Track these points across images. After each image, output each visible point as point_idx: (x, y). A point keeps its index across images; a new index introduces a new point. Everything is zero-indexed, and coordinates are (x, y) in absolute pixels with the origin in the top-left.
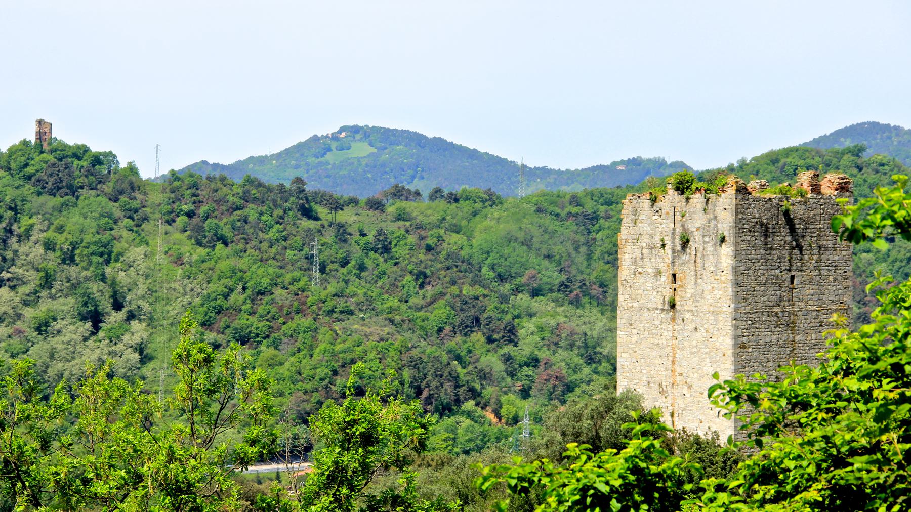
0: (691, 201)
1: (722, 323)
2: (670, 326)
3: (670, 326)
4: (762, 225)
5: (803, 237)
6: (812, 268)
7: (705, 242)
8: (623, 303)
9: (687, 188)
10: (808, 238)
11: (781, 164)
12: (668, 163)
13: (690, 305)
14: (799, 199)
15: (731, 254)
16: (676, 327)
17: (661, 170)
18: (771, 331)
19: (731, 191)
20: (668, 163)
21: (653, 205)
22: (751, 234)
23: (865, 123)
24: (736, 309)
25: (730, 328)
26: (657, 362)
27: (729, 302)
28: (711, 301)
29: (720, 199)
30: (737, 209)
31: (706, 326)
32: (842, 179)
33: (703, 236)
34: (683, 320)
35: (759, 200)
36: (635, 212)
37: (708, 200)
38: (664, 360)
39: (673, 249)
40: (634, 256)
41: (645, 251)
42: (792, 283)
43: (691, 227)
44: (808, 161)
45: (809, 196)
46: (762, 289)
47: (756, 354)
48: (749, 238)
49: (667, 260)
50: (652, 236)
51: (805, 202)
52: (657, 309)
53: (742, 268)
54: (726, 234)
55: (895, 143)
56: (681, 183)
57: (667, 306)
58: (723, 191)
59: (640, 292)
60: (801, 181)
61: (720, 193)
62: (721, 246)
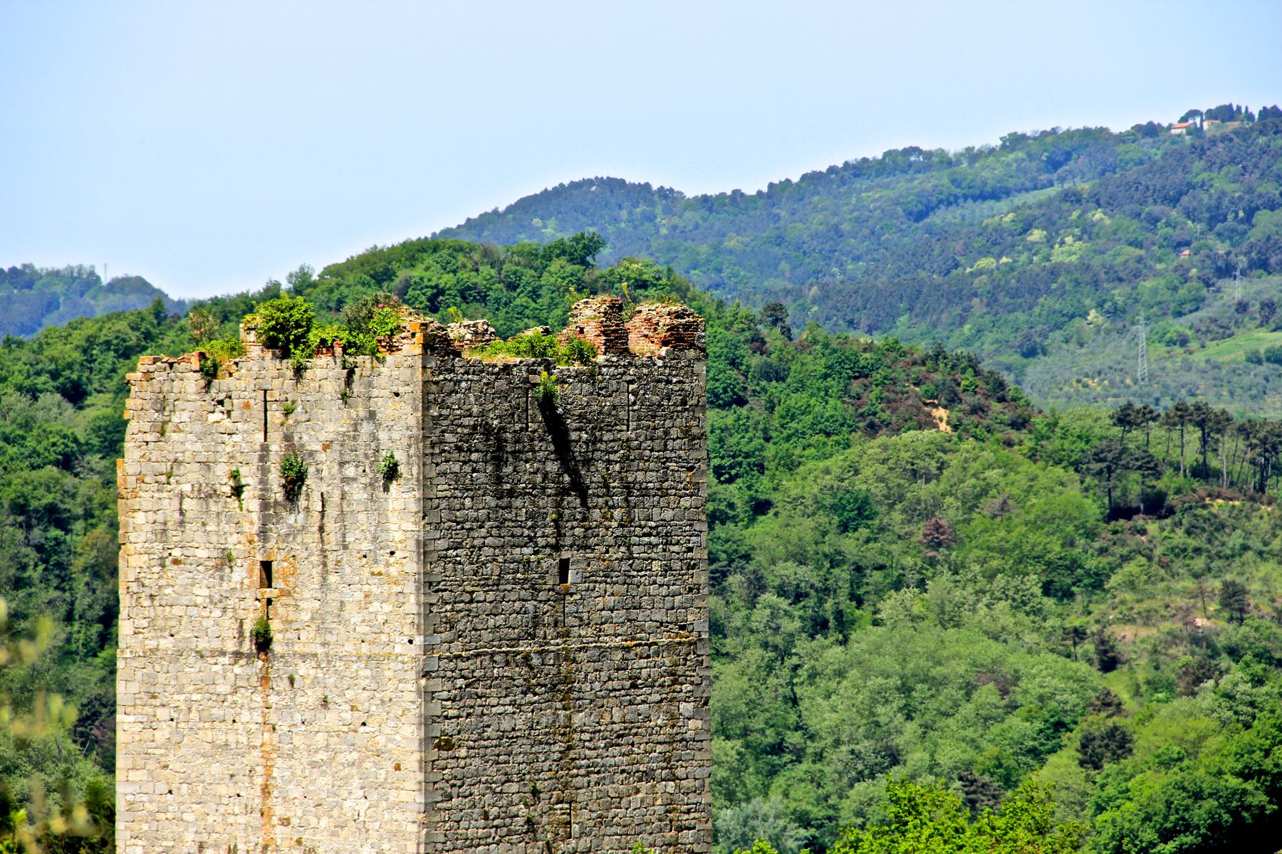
0: (308, 374)
1: (391, 686)
2: (257, 698)
3: (257, 698)
4: (488, 431)
5: (588, 462)
6: (610, 540)
7: (346, 480)
8: (132, 641)
9: (297, 341)
10: (601, 465)
11: (397, 282)
12: (105, 279)
13: (309, 641)
14: (577, 366)
15: (413, 507)
16: (273, 699)
17: (87, 298)
18: (512, 704)
19: (411, 349)
20: (105, 279)
21: (208, 386)
22: (463, 456)
23: (589, 182)
24: (428, 649)
25: (413, 696)
26: (222, 790)
27: (409, 631)
28: (363, 629)
29: (384, 370)
30: (426, 393)
31: (349, 694)
32: (679, 315)
33: (342, 464)
34: (292, 681)
35: (480, 369)
36: (161, 405)
37: (351, 373)
38: (243, 786)
39: (262, 498)
40: (160, 517)
41: (188, 504)
42: (563, 578)
43: (310, 440)
44: (463, 275)
45: (601, 359)
46: (491, 596)
47: (477, 761)
48: (456, 468)
49: (246, 527)
50: (207, 465)
51: (592, 375)
52: (223, 653)
53: (442, 544)
54: (400, 456)
55: (664, 231)
56: (282, 327)
57: (248, 646)
58: (392, 349)
59: (177, 611)
60: (581, 321)
61: (383, 353)
62: (386, 489)
